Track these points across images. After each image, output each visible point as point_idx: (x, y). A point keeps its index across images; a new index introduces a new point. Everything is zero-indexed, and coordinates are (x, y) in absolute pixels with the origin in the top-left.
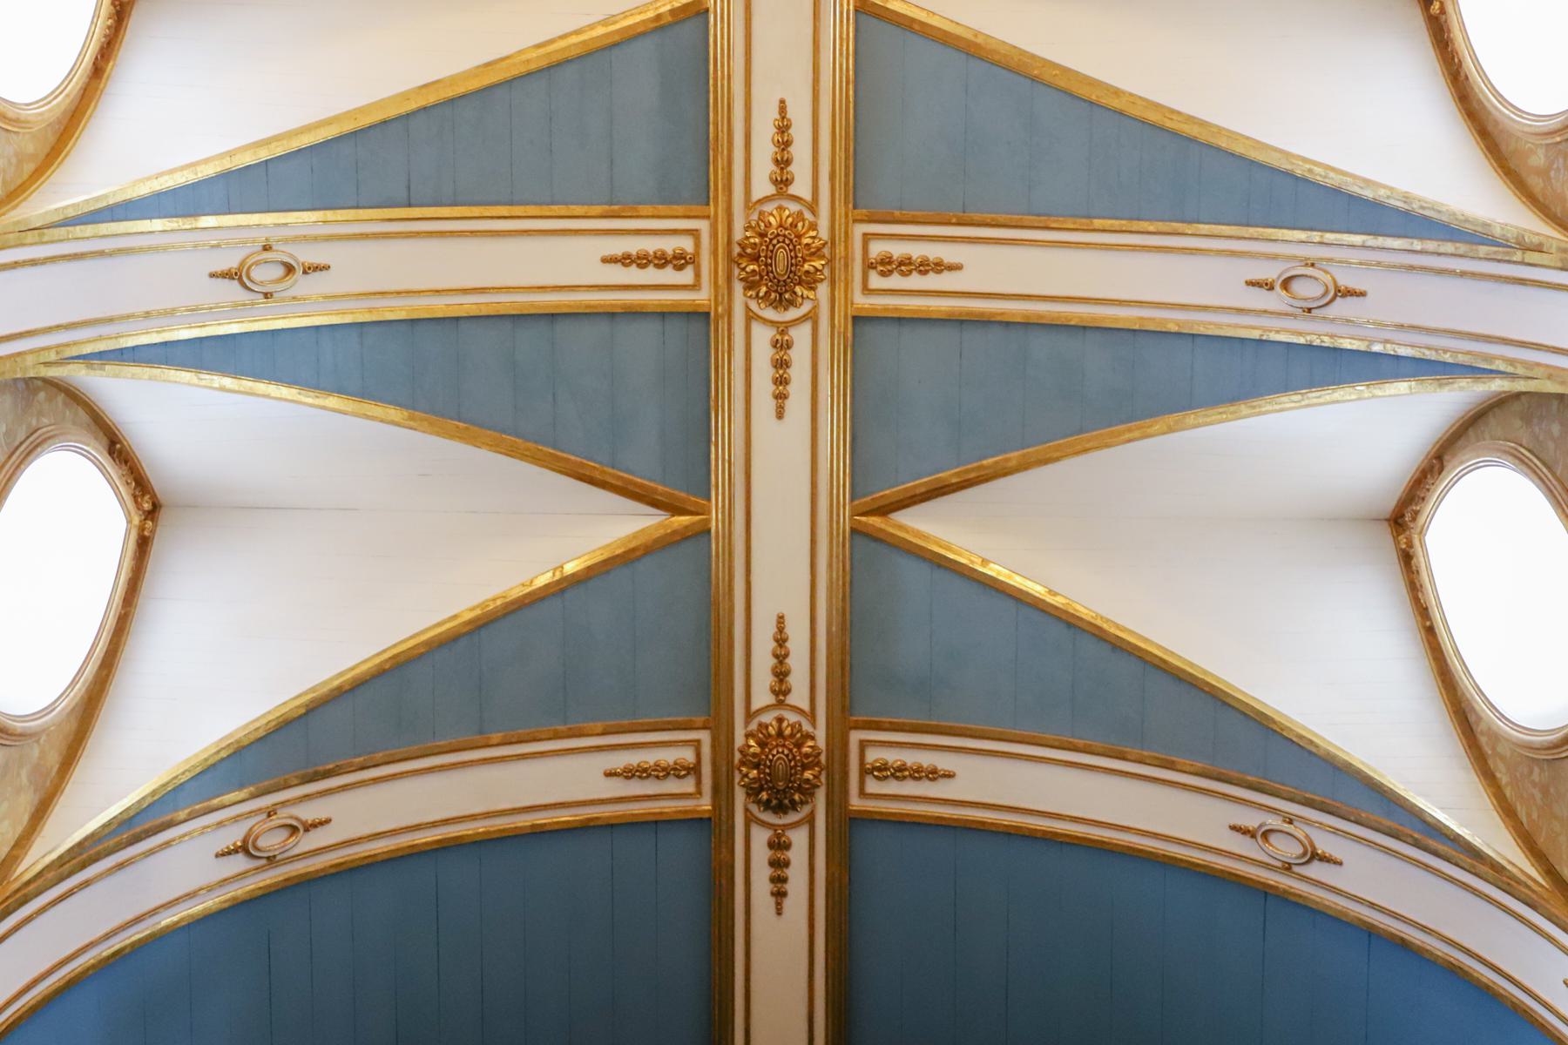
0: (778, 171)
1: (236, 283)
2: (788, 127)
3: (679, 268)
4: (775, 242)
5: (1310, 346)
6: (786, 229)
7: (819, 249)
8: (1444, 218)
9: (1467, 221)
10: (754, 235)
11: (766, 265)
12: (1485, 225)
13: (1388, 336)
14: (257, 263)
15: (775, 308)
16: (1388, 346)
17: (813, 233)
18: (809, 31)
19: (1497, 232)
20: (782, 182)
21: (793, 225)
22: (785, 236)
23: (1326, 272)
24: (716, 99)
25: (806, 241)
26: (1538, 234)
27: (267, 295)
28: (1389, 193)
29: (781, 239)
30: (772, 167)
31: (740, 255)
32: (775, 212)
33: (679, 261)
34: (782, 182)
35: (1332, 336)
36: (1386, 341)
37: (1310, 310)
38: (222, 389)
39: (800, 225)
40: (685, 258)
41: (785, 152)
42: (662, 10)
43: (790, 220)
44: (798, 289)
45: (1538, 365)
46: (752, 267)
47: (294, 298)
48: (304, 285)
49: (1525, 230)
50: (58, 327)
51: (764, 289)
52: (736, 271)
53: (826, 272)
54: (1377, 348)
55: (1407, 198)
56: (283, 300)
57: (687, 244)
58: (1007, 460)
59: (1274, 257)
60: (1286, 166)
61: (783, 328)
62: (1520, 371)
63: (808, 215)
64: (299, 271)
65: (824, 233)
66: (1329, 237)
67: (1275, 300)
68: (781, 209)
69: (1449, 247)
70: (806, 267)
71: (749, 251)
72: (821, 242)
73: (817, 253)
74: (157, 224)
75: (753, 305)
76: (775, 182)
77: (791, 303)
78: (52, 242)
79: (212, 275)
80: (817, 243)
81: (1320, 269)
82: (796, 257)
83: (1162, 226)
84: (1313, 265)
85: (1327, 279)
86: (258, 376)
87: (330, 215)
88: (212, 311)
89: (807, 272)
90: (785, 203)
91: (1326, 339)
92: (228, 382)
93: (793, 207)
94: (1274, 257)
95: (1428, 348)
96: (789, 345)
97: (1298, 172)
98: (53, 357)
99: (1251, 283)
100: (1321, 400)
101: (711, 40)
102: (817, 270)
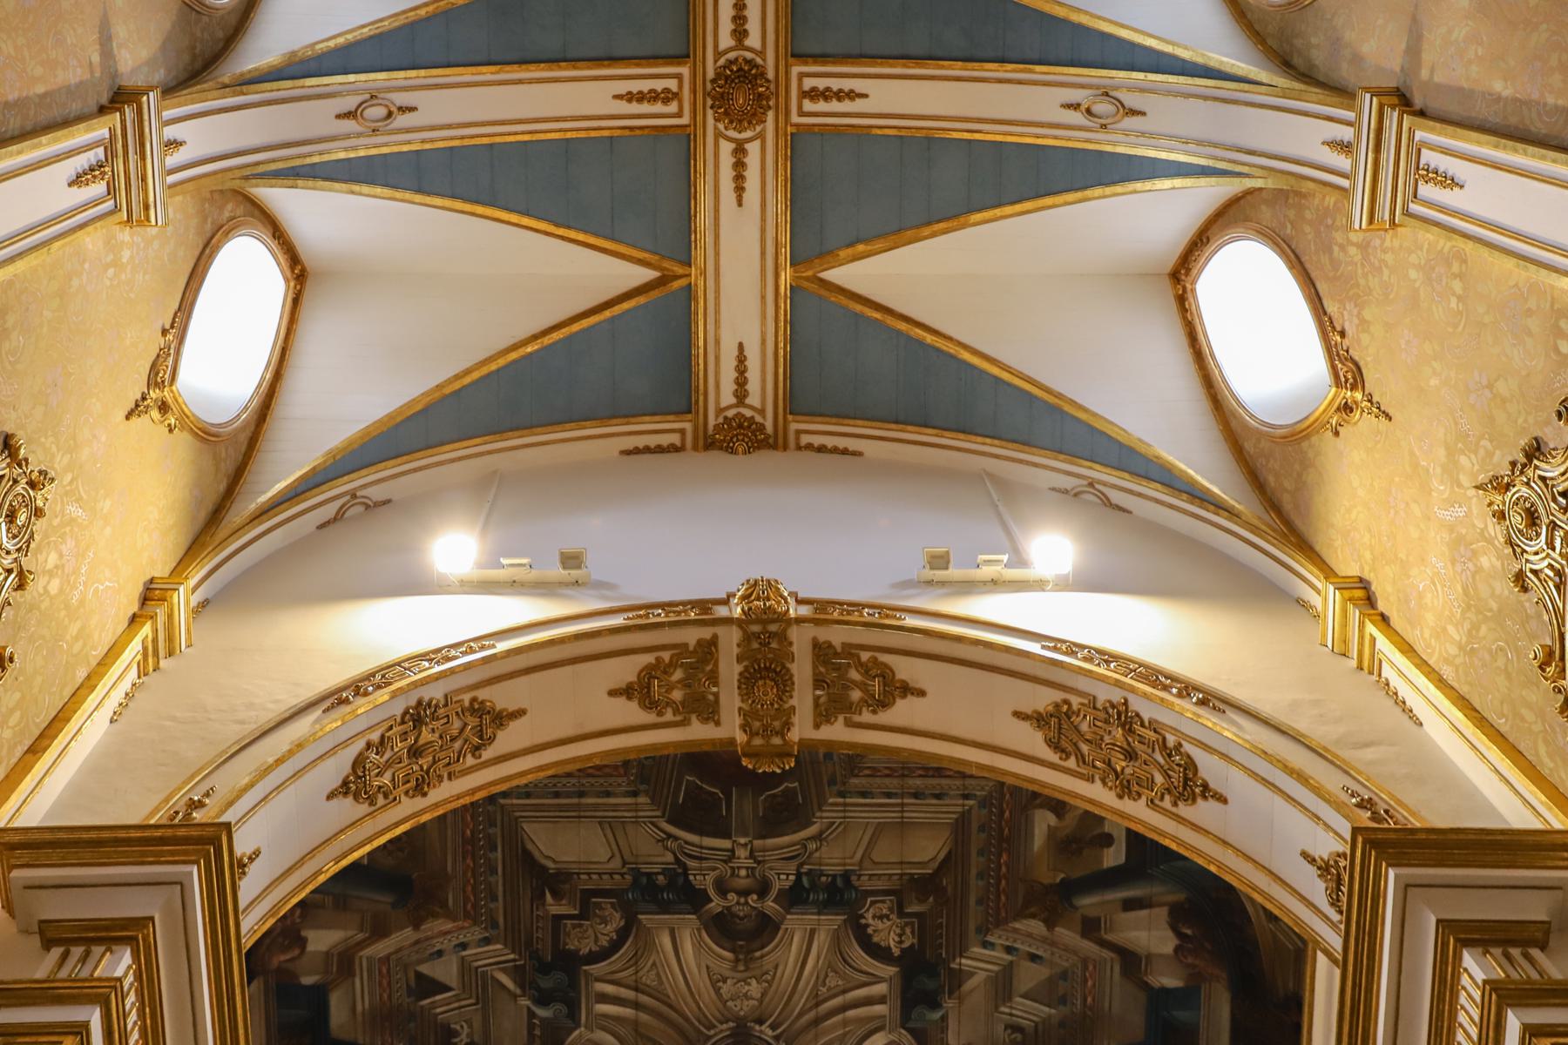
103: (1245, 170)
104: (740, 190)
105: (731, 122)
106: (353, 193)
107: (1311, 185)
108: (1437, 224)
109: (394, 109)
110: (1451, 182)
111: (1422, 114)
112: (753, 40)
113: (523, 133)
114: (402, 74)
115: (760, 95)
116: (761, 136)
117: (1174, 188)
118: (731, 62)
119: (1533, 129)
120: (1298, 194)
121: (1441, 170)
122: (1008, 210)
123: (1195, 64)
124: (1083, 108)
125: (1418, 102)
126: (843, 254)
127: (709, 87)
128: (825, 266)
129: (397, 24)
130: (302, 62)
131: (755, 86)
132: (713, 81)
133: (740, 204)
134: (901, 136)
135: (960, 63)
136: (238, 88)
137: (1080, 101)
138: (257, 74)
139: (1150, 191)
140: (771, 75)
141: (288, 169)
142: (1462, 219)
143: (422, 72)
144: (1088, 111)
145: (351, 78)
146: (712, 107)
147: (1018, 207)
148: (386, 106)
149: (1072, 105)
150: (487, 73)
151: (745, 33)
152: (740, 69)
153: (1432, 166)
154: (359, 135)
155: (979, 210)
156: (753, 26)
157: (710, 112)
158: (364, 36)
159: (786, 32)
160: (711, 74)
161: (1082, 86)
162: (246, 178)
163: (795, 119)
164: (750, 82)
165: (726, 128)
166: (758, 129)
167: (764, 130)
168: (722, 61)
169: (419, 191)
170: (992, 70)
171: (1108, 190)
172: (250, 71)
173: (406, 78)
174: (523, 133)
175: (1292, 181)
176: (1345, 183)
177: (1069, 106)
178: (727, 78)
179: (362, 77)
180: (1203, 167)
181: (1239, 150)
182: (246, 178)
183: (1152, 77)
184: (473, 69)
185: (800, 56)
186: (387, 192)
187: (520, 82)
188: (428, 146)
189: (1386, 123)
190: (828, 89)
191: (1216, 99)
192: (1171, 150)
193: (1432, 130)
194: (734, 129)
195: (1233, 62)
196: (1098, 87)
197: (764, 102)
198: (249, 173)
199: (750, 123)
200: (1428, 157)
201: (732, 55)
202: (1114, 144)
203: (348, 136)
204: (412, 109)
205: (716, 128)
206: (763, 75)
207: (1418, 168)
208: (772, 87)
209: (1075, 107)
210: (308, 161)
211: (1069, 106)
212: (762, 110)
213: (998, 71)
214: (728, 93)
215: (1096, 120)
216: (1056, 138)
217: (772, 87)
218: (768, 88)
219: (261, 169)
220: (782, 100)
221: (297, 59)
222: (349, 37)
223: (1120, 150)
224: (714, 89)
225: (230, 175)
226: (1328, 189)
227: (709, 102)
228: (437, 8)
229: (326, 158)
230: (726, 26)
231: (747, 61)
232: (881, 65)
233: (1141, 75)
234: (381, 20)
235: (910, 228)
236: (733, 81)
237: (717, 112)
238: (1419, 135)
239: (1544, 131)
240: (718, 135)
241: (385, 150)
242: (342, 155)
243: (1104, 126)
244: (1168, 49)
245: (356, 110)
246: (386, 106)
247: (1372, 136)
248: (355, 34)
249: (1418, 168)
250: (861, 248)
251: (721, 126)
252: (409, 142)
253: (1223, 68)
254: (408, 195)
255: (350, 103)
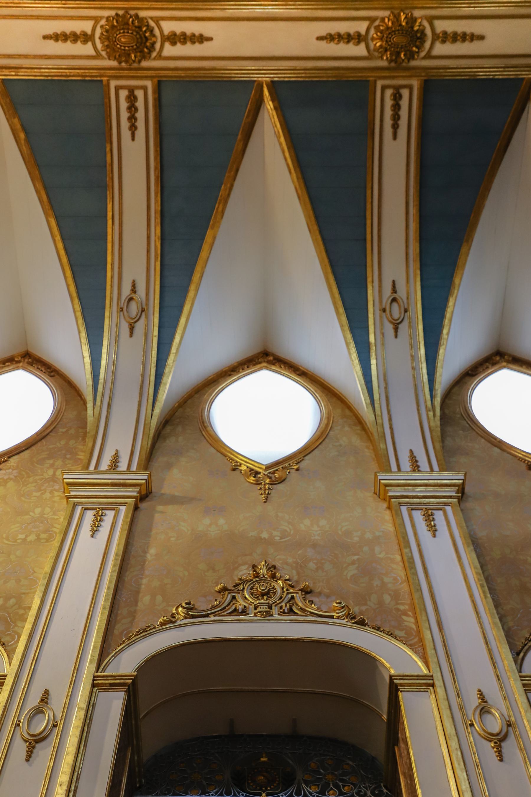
0: (353, 41)
1: (400, 326)
2: (330, 35)
3: (401, 97)
4: (390, 43)
6: (383, 36)
7: (395, 16)
10: (386, 55)
11: (402, 48)
14: (391, 315)
15: (424, 42)
17: (386, 20)
18: (281, 24)
20: (358, 38)
21: (381, 32)
22: (387, 37)
24: (316, 77)
25: (390, 24)
27: (406, 311)
29: (389, 40)
30: (351, 45)
31: (396, 62)
32: (374, 43)
33: (397, 97)
34: (358, 38)
38: (448, 334)
39: (381, 28)
40: (396, 94)
41: (343, 37)
42: (272, 106)
43: (379, 34)
44: (416, 28)
46: (402, 56)
47: (408, 298)
48: (402, 293)
50: (418, 410)
51: (414, 49)
52: (404, 64)
53: (407, 11)
56: (408, 304)
57: (389, 93)
61: (436, 37)
63: (377, 23)
64: (395, 295)
65: (387, 13)
68: (373, 39)
70: (404, 24)
71: (394, 58)
72: (391, 15)
73: (397, 17)
74: (373, 362)
75: (422, 54)
76: (358, 43)
77: (423, 32)
78: (381, 411)
79: (396, 336)
80: (391, 17)
82: (398, 30)
86: (443, 316)
87: (369, 280)
88: (412, 338)
89: (407, 23)
90: (370, 36)
92: (445, 331)
93: (372, 31)
96: (445, 33)
98: (431, 414)
101: (286, 79)
102: (406, 18)
103: (98, 403)
104: (55, 37)
105: (107, 31)
107: (90, 444)
108: (69, 524)
110: (95, 530)
111: (136, 508)
112: (169, 50)
115: (129, 55)
116: (98, 56)
117: (83, 358)
118: (152, 31)
119: (128, 573)
120: (84, 439)
121: (102, 523)
122: (60, 245)
123: (164, 367)
124: (133, 295)
125: (143, 506)
126: (16, 121)
127: (132, 12)
128: (5, 107)
131: (135, 51)
132: (137, 16)
133: (45, 37)
134: (106, 166)
135: (159, 209)
137: (137, 293)
139: (81, 342)
140: (145, 64)
142: (72, 538)
144: (131, 299)
146: (117, 15)
147: (62, 252)
149: (135, 288)
151: (174, 44)
152: (147, 39)
153: (104, 518)
155: (58, 225)
156: (179, 50)
157: (113, 13)
159: (175, 77)
160: (142, 14)
161: (147, 294)
163: (113, 83)
164: (138, 47)
165: (102, 27)
166: (104, 53)
167: (103, 58)
168: (152, 24)
170: (156, 231)
171: (79, 314)
175: (93, 433)
176: (92, 467)
177: (134, 285)
178: (140, 28)
180: (99, 376)
181: (111, 399)
183: (155, 340)
185: (159, 87)
189: (130, 489)
190: (136, 109)
191: (143, 382)
192: (109, 354)
193: (126, 516)
194: (102, 34)
195: (166, 391)
196: (147, 304)
197: (123, 59)
199: (108, 46)
200: (110, 515)
201: (157, 32)
202: (110, 317)
205: (101, 18)
206: (144, 57)
207: (103, 509)
208: (135, 65)
209: (134, 290)
211: (134, 285)
212: (117, 57)
213: (155, 236)
214: (128, 29)
215: (126, 304)
216: (112, 277)
217: (135, 65)
218: (134, 61)
220: (126, 73)
223: (107, 322)
224: (131, 17)
226: (89, 456)
227: (121, 12)
230: (178, 27)
231: (153, 44)
232: (156, 151)
233: (156, 333)
235: (40, 173)
236: (137, 33)
237: (113, 19)
238: (123, 508)
239: (126, 579)
240: (96, 19)
243: (122, 310)
244: (174, 350)
247: (122, 481)
249: (103, 509)
250: (22, 136)
251: (103, 22)
253: (162, 385)
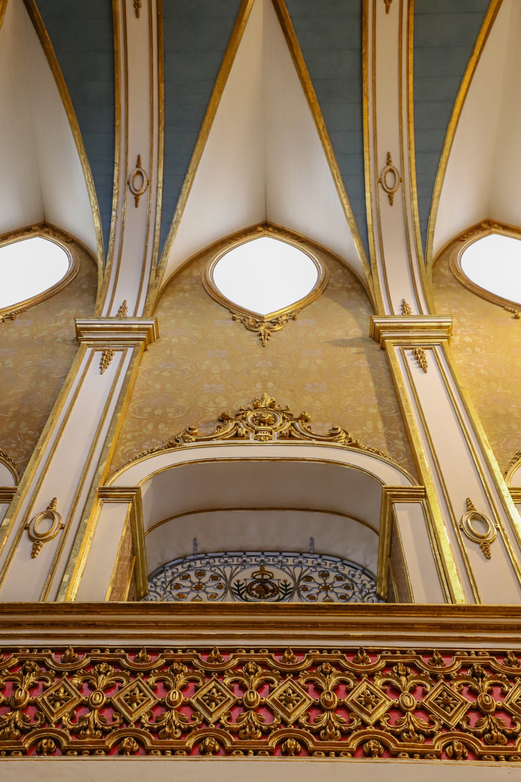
5: (113, 184)
8: (169, 238)
9: (168, 247)
12: (167, 254)
13: (119, 217)
16: (115, 218)
19: (164, 259)
23: (145, 190)
26: (163, 275)
28: (179, 214)
35: (118, 194)
36: (117, 217)
37: (128, 184)
45: (109, 278)
49: (165, 270)
54: (114, 213)
55: (178, 222)
58: (49, 44)
59: (151, 167)
60: (190, 170)
62: (106, 271)
66: (160, 191)
67: (132, 168)
69: (157, 240)
81: (146, 187)
83: (162, 115)
84: (148, 184)
85: (142, 191)
91: (116, 191)
94: (151, 167)
95: (115, 234)
97: (188, 176)
99: (139, 157)
100: (90, 191)
106: (439, 196)
109: (388, 168)
113: (408, 80)
114: (366, 162)
129: (335, 165)
130: (357, 226)
136: (372, 266)
138: (364, 255)
141: (422, 237)
143: (366, 148)
145: (368, 195)
148: (386, 173)
150: (368, 105)
154: (403, 191)
158: (343, 186)
162: (426, 263)
169: (441, 152)
172: (362, 258)
173: (369, 160)
174: (408, 80)
179: (367, 188)
182: (426, 263)
184: (365, 114)
186: (440, 173)
187: (374, 82)
188: (413, 146)
198: (423, 262)
203: (404, 199)
204: (389, 156)
210: (418, 225)
219: (421, 254)
221: (356, 229)
222: (343, 195)
225: (424, 273)
228: (326, 138)
229: (416, 213)
234: (333, 174)
241: (414, 174)
242: (415, 202)
245: (388, 192)
246: (386, 173)
248: (341, 191)
252: (410, 158)
254: (443, 160)
255: (383, 196)
